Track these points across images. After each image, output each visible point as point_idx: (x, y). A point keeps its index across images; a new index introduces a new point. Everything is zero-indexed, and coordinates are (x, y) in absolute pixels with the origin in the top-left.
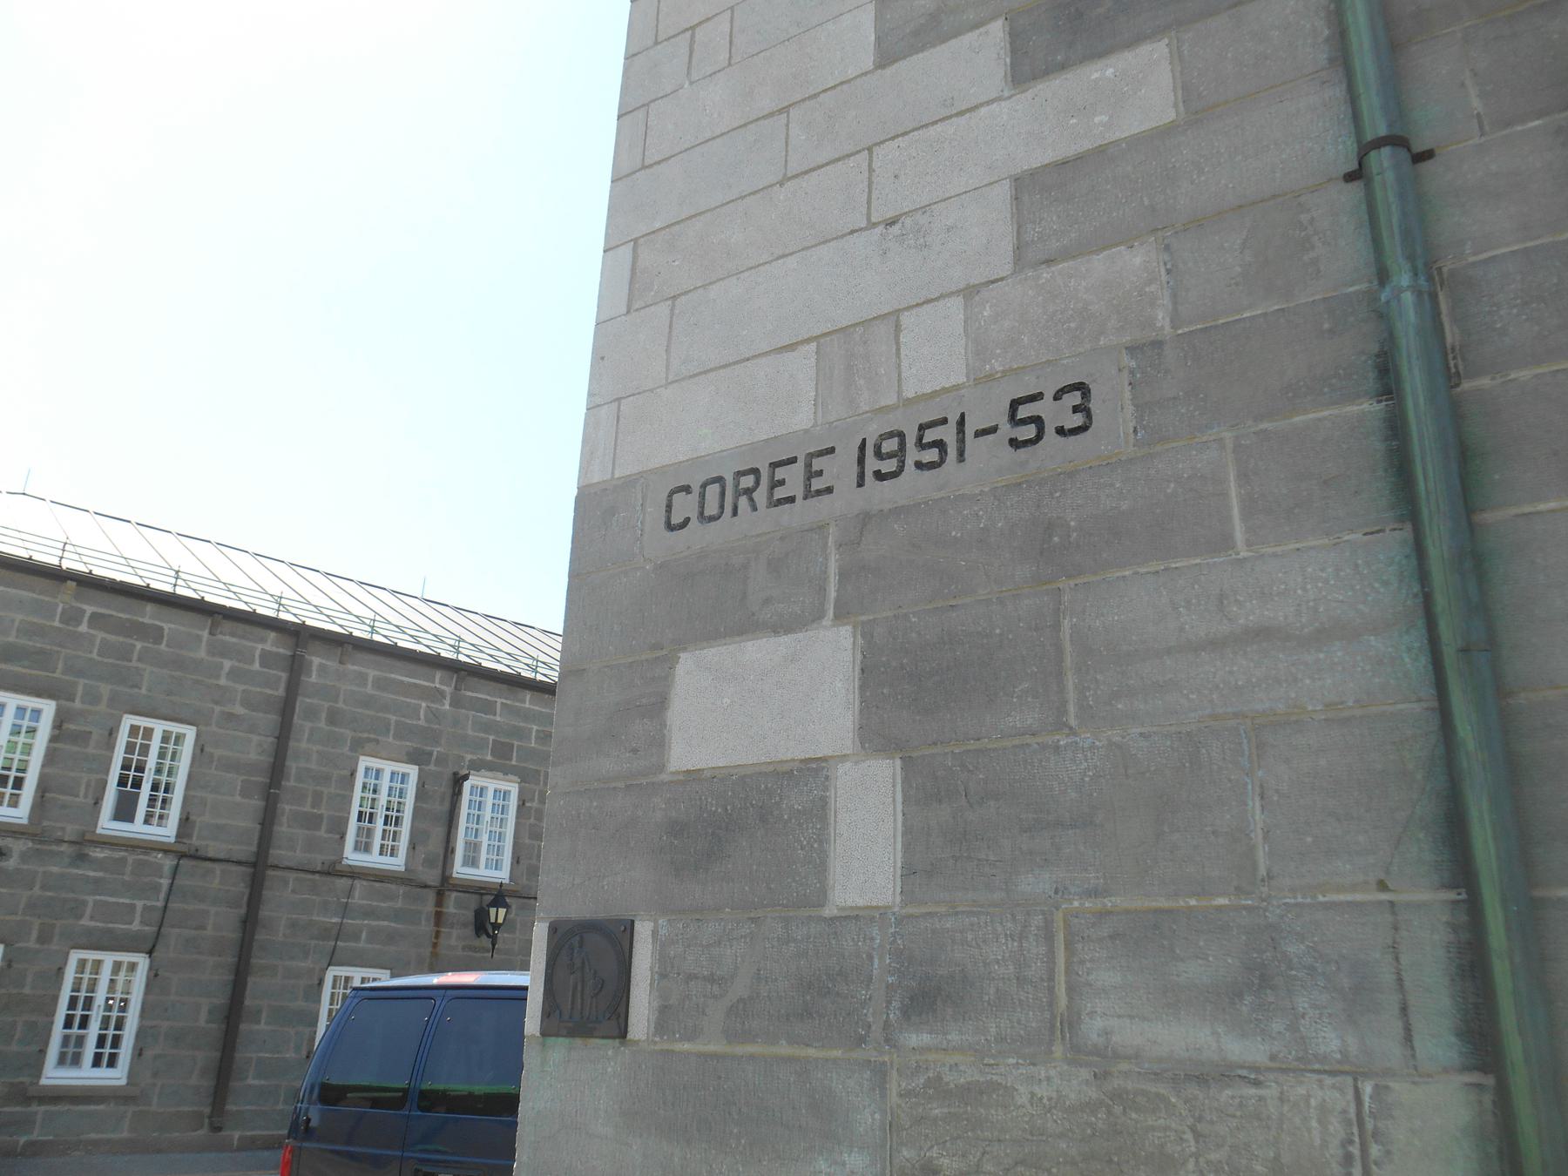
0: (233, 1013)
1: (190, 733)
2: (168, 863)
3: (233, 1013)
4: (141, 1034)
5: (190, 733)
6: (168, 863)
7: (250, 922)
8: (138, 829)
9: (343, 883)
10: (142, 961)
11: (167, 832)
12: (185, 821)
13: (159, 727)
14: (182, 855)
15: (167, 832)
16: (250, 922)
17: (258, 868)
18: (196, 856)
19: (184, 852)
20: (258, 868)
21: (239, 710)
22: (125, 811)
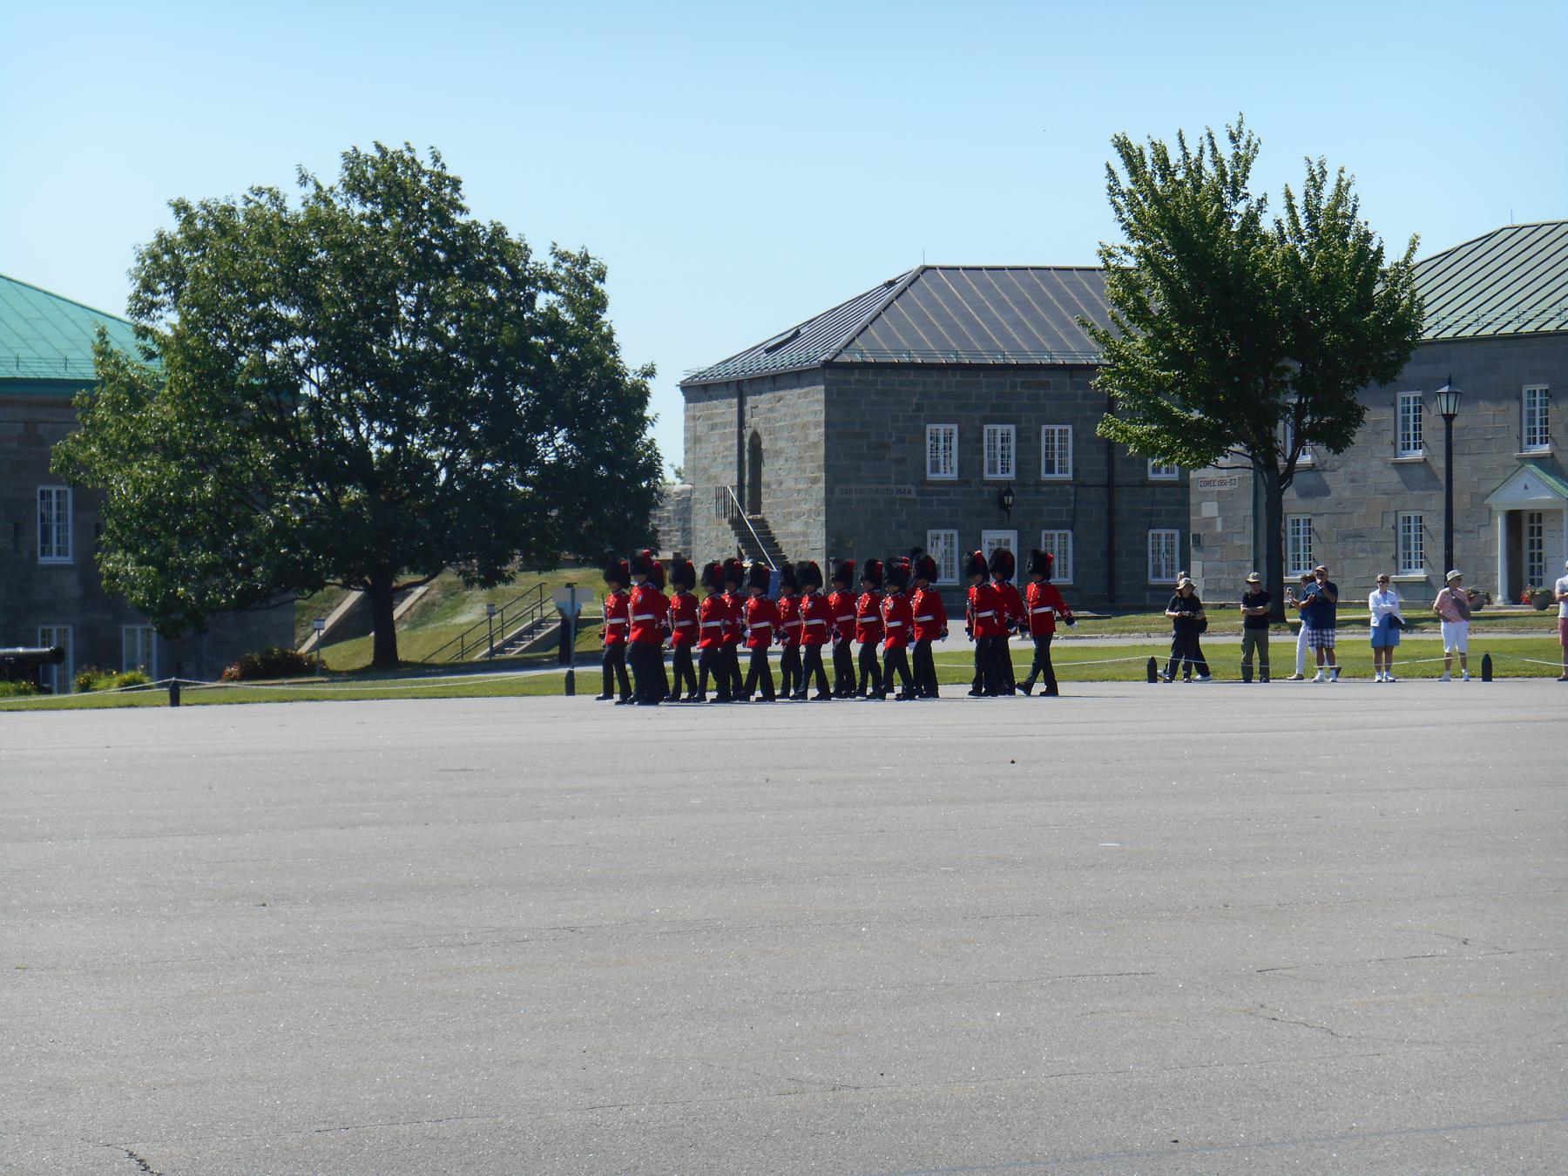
0: (1110, 553)
1: (1070, 428)
2: (1072, 490)
3: (1110, 553)
4: (1075, 564)
5: (1070, 428)
6: (1072, 490)
7: (1111, 512)
8: (1056, 476)
9: (1149, 490)
10: (1069, 533)
11: (1069, 476)
12: (1075, 470)
13: (1056, 428)
14: (1077, 486)
15: (1069, 476)
16: (1111, 512)
17: (1110, 486)
18: (1083, 485)
19: (1077, 483)
20: (1110, 486)
21: (1088, 414)
22: (1050, 470)
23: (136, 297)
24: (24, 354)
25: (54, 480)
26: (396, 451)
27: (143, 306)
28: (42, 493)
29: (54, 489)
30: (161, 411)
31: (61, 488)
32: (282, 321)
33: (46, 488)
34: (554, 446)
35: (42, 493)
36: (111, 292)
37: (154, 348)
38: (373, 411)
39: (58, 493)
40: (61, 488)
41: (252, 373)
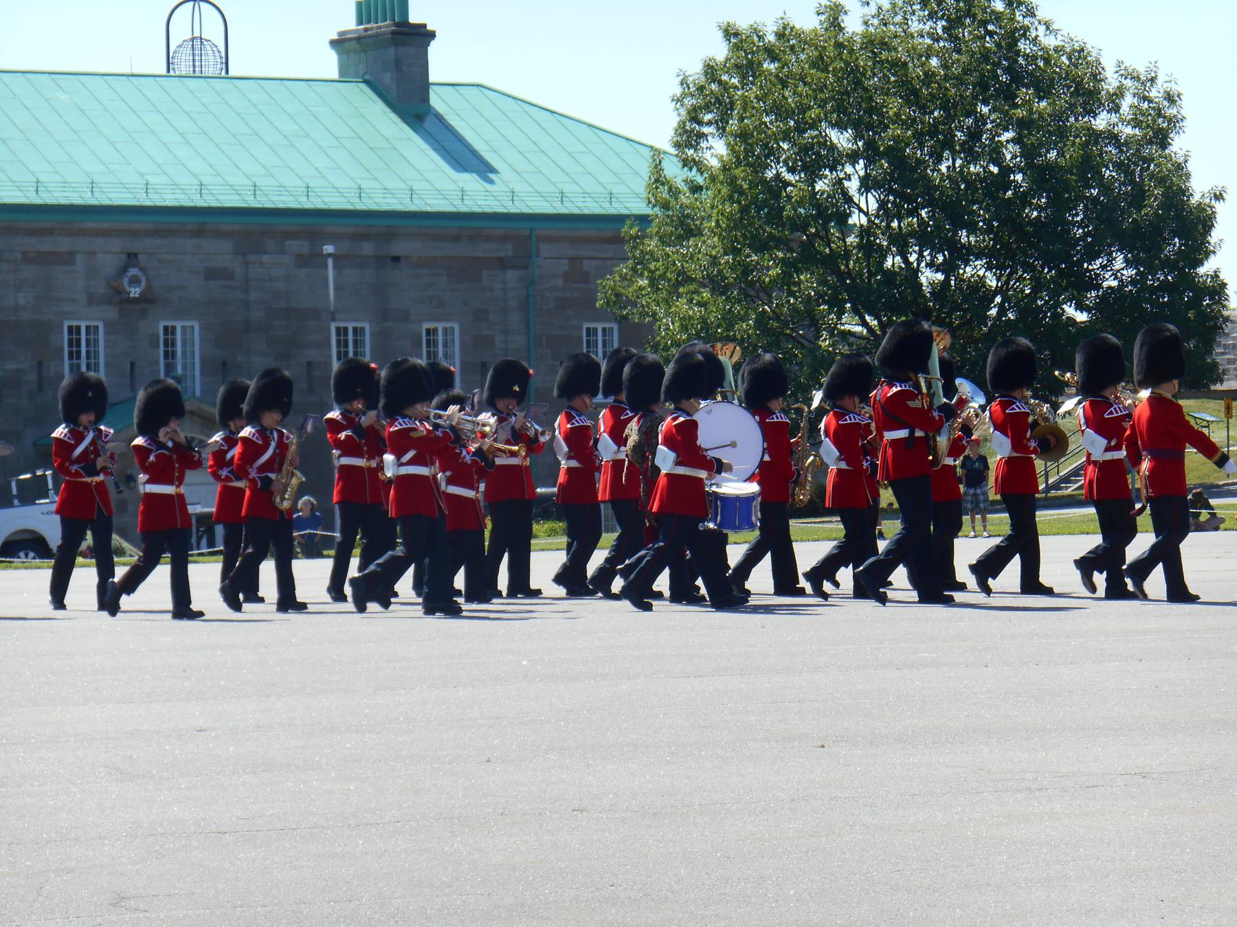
23: (682, 129)
24: (569, 188)
25: (600, 316)
26: (947, 279)
27: (688, 138)
28: (588, 330)
29: (600, 327)
30: (709, 245)
31: (607, 325)
32: (833, 147)
33: (592, 325)
34: (1115, 271)
35: (588, 330)
36: (659, 126)
37: (700, 180)
38: (924, 238)
39: (604, 330)
40: (607, 325)
41: (800, 203)
